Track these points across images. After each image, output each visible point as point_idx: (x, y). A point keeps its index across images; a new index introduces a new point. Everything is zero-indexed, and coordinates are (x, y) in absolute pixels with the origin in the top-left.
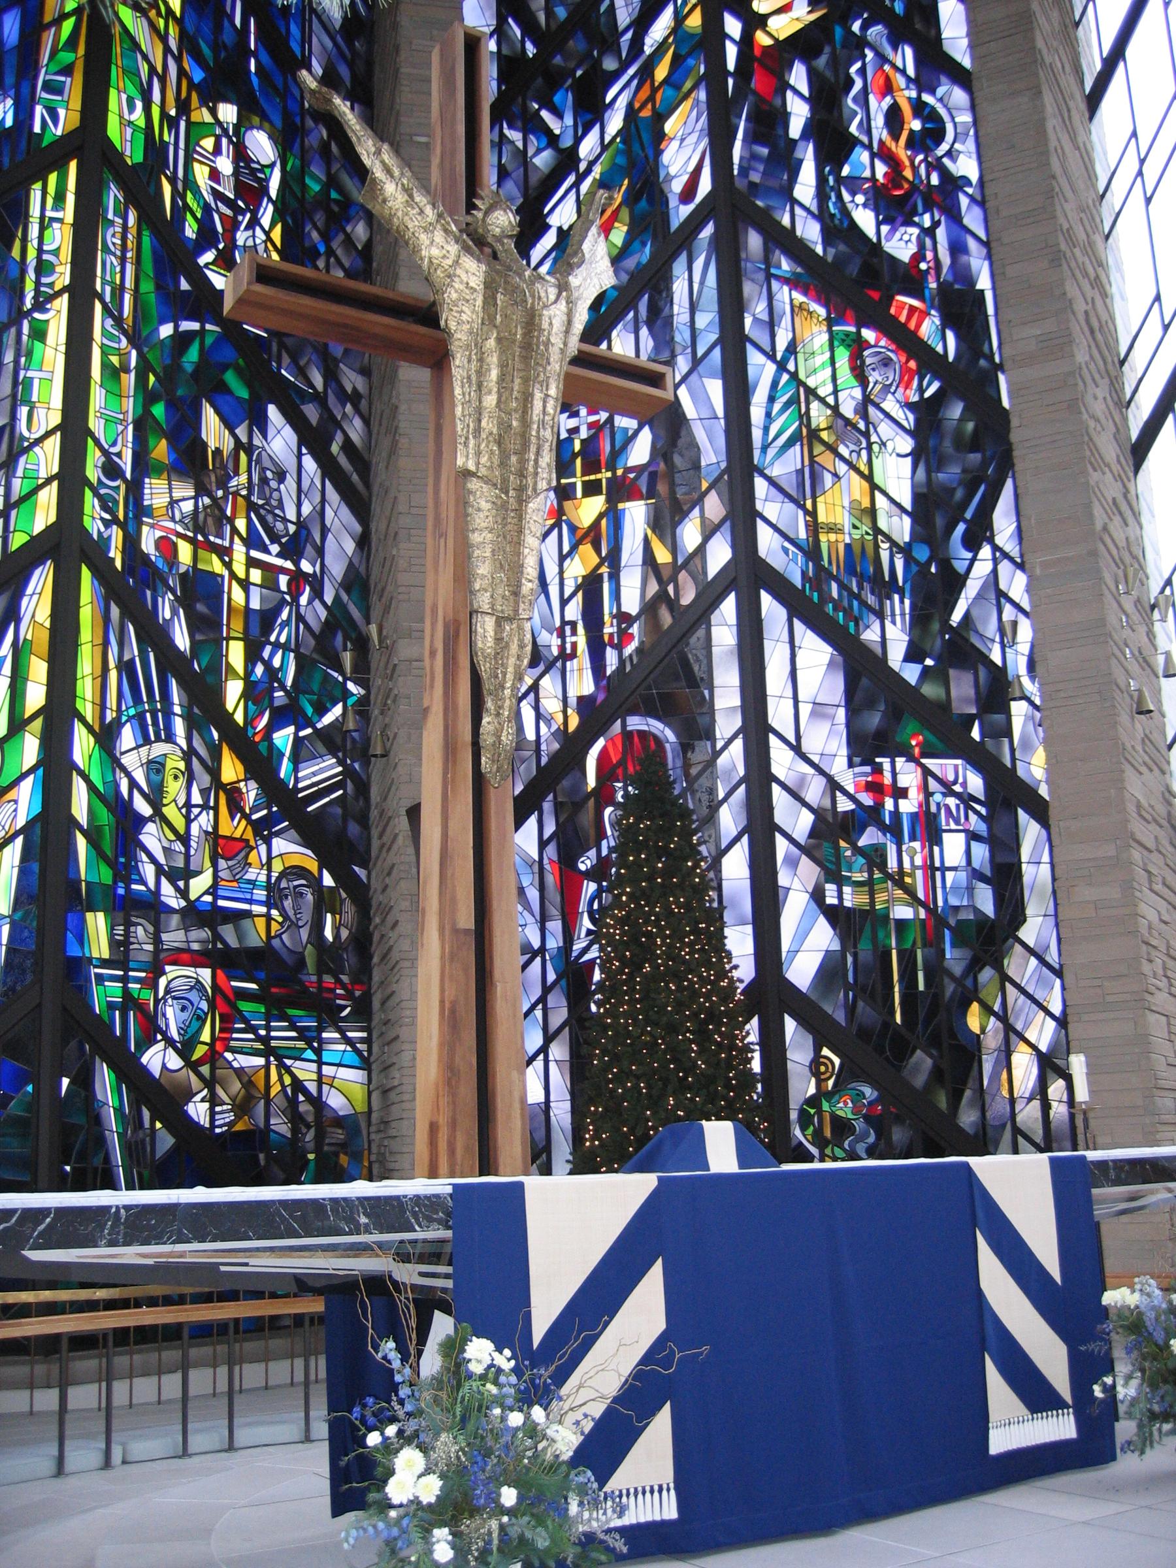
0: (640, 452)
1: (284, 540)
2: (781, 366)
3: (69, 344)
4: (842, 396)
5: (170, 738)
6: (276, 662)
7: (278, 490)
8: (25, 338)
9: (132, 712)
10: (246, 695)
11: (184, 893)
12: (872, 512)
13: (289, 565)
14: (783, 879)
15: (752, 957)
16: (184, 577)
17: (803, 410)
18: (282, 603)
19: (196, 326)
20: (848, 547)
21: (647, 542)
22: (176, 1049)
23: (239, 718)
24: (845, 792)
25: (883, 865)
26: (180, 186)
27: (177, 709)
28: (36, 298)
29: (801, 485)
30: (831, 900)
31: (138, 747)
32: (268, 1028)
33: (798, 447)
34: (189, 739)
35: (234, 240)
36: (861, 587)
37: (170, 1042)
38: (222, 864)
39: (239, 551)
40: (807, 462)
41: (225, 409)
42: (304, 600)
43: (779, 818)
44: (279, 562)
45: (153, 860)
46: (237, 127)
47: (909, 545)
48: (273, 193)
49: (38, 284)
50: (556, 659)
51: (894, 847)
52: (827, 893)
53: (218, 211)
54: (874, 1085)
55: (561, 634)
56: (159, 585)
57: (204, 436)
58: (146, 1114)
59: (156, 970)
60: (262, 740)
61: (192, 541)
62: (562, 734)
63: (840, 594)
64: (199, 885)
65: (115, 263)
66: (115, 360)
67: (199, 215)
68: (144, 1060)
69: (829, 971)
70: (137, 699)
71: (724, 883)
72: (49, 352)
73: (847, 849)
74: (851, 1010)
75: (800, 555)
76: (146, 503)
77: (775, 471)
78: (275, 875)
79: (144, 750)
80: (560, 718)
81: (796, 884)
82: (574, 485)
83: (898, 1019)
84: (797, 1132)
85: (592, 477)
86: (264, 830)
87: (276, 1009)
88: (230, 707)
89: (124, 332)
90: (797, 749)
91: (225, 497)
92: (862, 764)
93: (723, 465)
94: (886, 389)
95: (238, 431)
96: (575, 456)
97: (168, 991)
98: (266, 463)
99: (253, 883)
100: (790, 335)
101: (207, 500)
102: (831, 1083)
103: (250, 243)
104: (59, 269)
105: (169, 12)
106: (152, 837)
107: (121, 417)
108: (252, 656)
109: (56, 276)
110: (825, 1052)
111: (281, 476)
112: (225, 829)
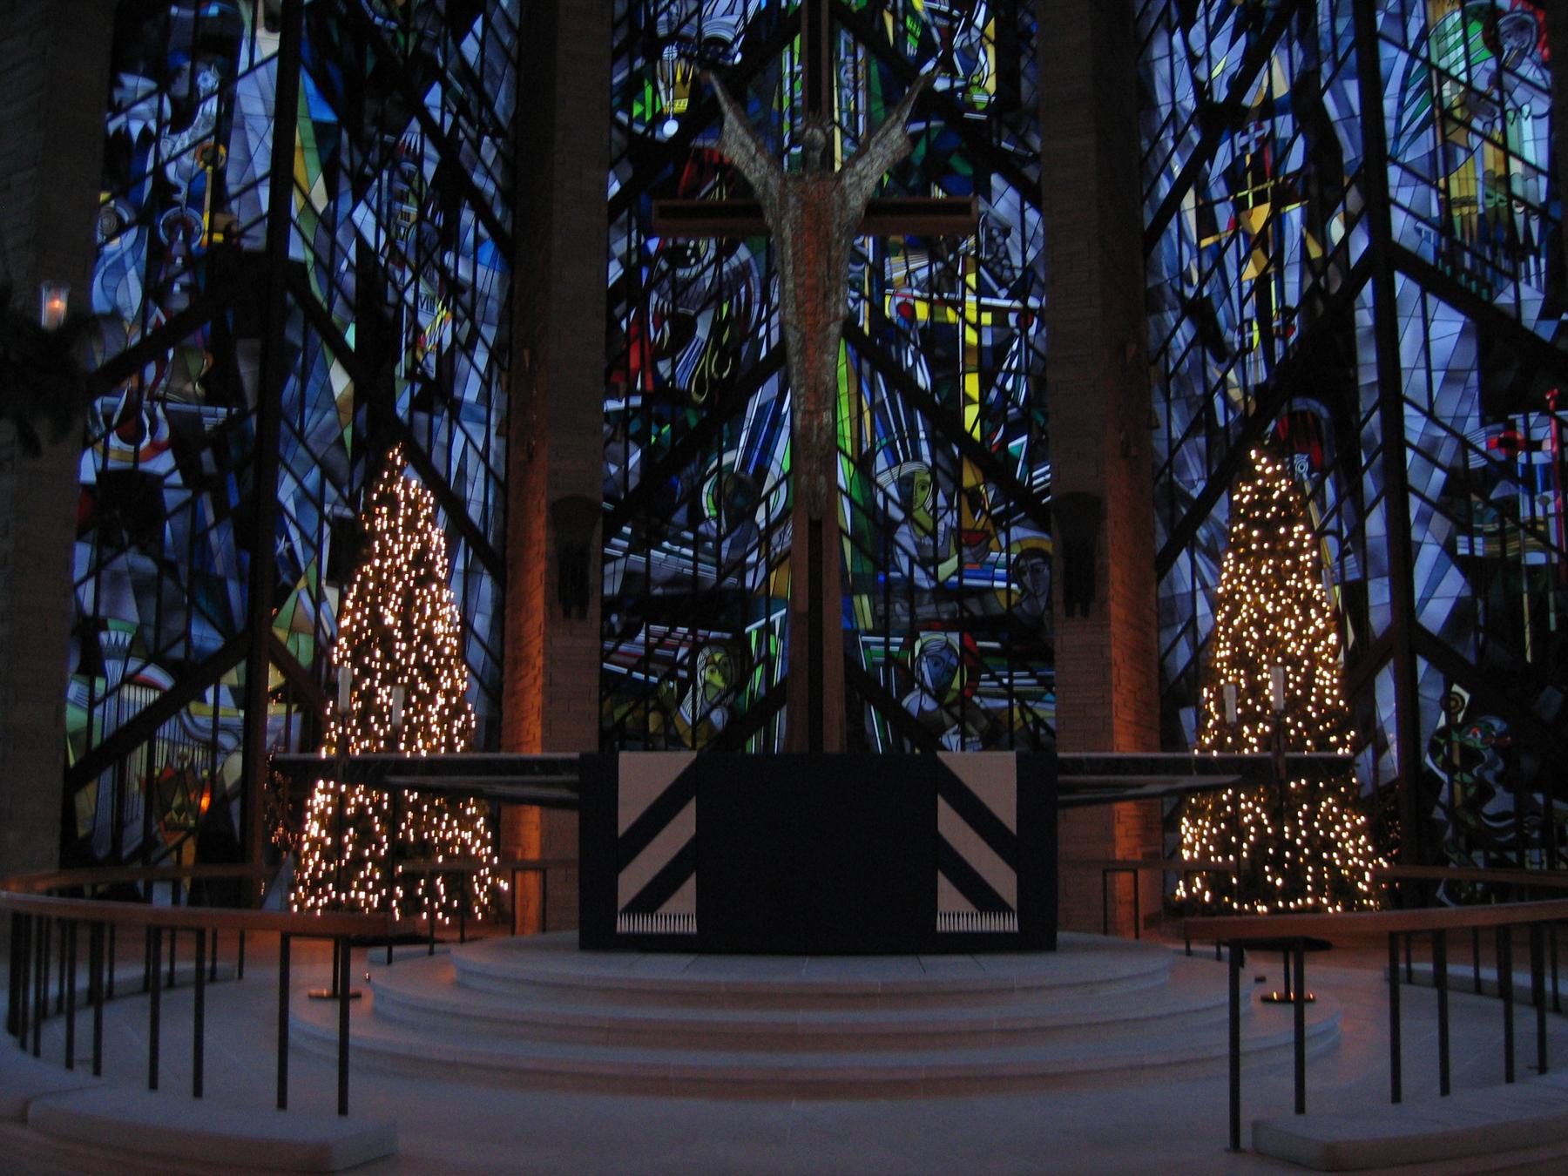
0: (1295, 160)
1: (1011, 285)
2: (1414, 55)
4: (1475, 71)
5: (917, 457)
6: (1009, 386)
7: (1004, 243)
9: (884, 442)
10: (981, 416)
11: (935, 577)
12: (1507, 179)
13: (1017, 304)
14: (1416, 534)
15: (1388, 608)
16: (923, 331)
17: (1435, 93)
18: (1011, 338)
19: (921, 126)
20: (1481, 217)
21: (1303, 241)
22: (930, 695)
23: (977, 434)
24: (1477, 451)
25: (1514, 514)
26: (900, 15)
27: (922, 435)
29: (1434, 164)
30: (1462, 551)
31: (890, 468)
32: (1011, 678)
33: (1430, 130)
34: (933, 456)
35: (952, 46)
36: (1494, 253)
37: (924, 689)
38: (966, 551)
39: (971, 300)
40: (1439, 142)
42: (1032, 331)
43: (1413, 479)
44: (1007, 303)
45: (906, 552)
47: (1546, 205)
50: (1238, 354)
51: (1527, 498)
52: (1459, 544)
53: (935, 25)
54: (1504, 718)
55: (1242, 333)
56: (902, 339)
58: (907, 744)
59: (912, 637)
60: (999, 449)
61: (929, 301)
62: (1244, 419)
63: (1473, 264)
64: (947, 569)
68: (905, 703)
69: (1461, 614)
70: (888, 432)
71: (1368, 542)
73: (1478, 503)
74: (1481, 651)
75: (1433, 232)
76: (887, 278)
77: (1408, 158)
78: (1013, 556)
79: (895, 470)
80: (1242, 405)
81: (1429, 538)
82: (1247, 196)
83: (1529, 658)
84: (1428, 760)
85: (1260, 187)
86: (1002, 522)
87: (1015, 658)
88: (968, 426)
90: (1430, 415)
91: (956, 260)
92: (1494, 423)
93: (1361, 160)
94: (1522, 54)
96: (1246, 171)
97: (922, 650)
98: (991, 223)
99: (995, 565)
100: (1422, 22)
101: (940, 265)
102: (1460, 717)
103: (966, 43)
106: (904, 536)
108: (985, 386)
110: (1456, 688)
111: (1006, 232)
112: (967, 525)
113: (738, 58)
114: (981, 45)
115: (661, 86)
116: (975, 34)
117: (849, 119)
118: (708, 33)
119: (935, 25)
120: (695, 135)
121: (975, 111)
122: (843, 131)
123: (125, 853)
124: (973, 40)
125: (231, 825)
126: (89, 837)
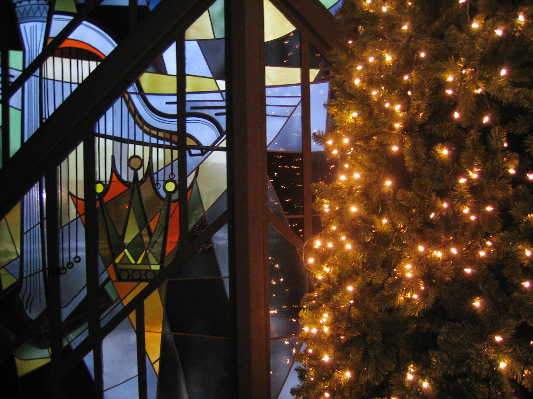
123: (66, 313)
125: (218, 272)
126: (16, 287)
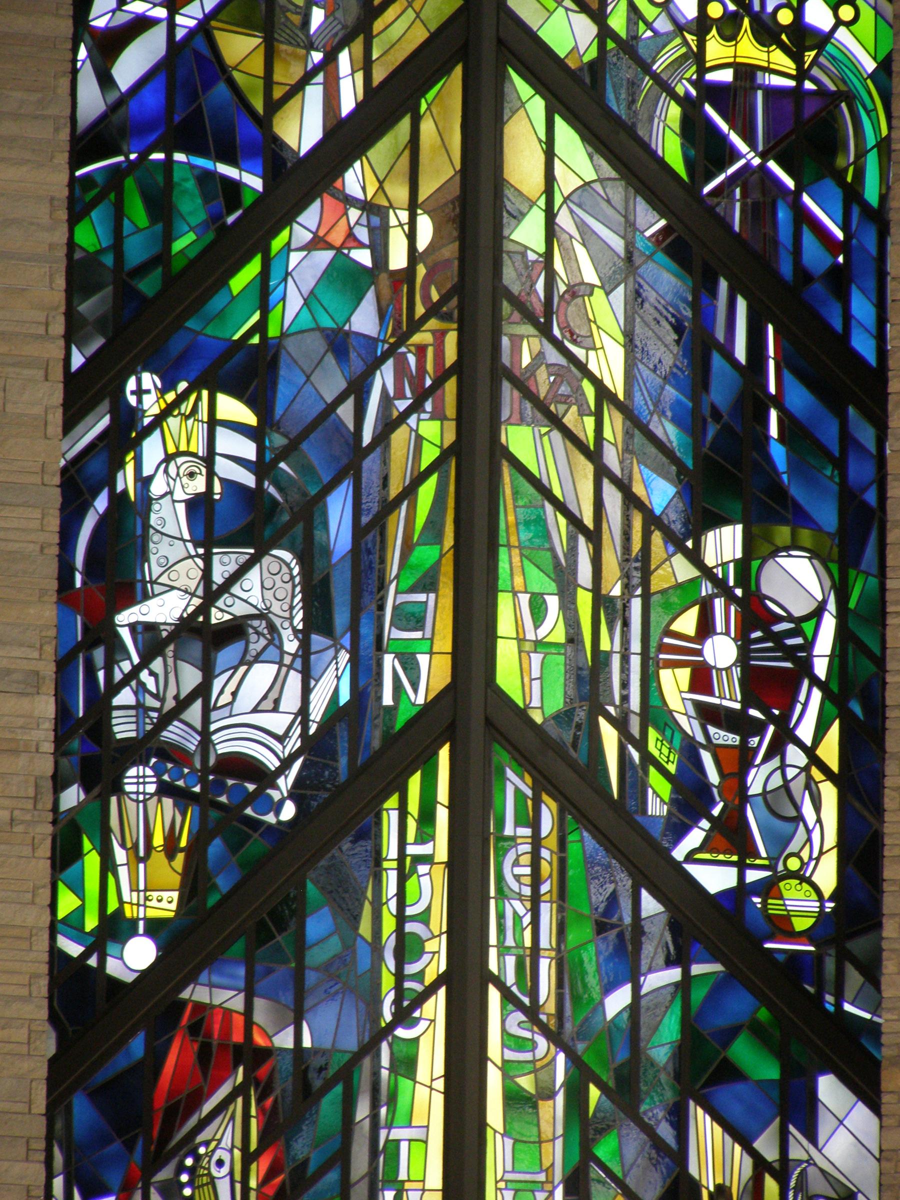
3: (448, 1076)
8: (385, 1073)
26: (635, 728)
28: (397, 1002)
35: (744, 788)
41: (736, 1112)
46: (743, 566)
48: (821, 668)
49: (400, 977)
53: (710, 746)
57: (693, 1170)
65: (521, 911)
66: (526, 1083)
67: (672, 768)
72: (421, 1093)
89: (545, 1030)
95: (757, 1145)
103: (776, 781)
104: (430, 946)
105: (603, 393)
107: (542, 1177)
109: (426, 958)
113: (289, 811)
114: (810, 786)
115: (120, 855)
116: (795, 756)
117: (520, 966)
118: (224, 745)
119: (710, 746)
120: (191, 978)
121: (791, 935)
122: (507, 995)
124: (791, 773)
